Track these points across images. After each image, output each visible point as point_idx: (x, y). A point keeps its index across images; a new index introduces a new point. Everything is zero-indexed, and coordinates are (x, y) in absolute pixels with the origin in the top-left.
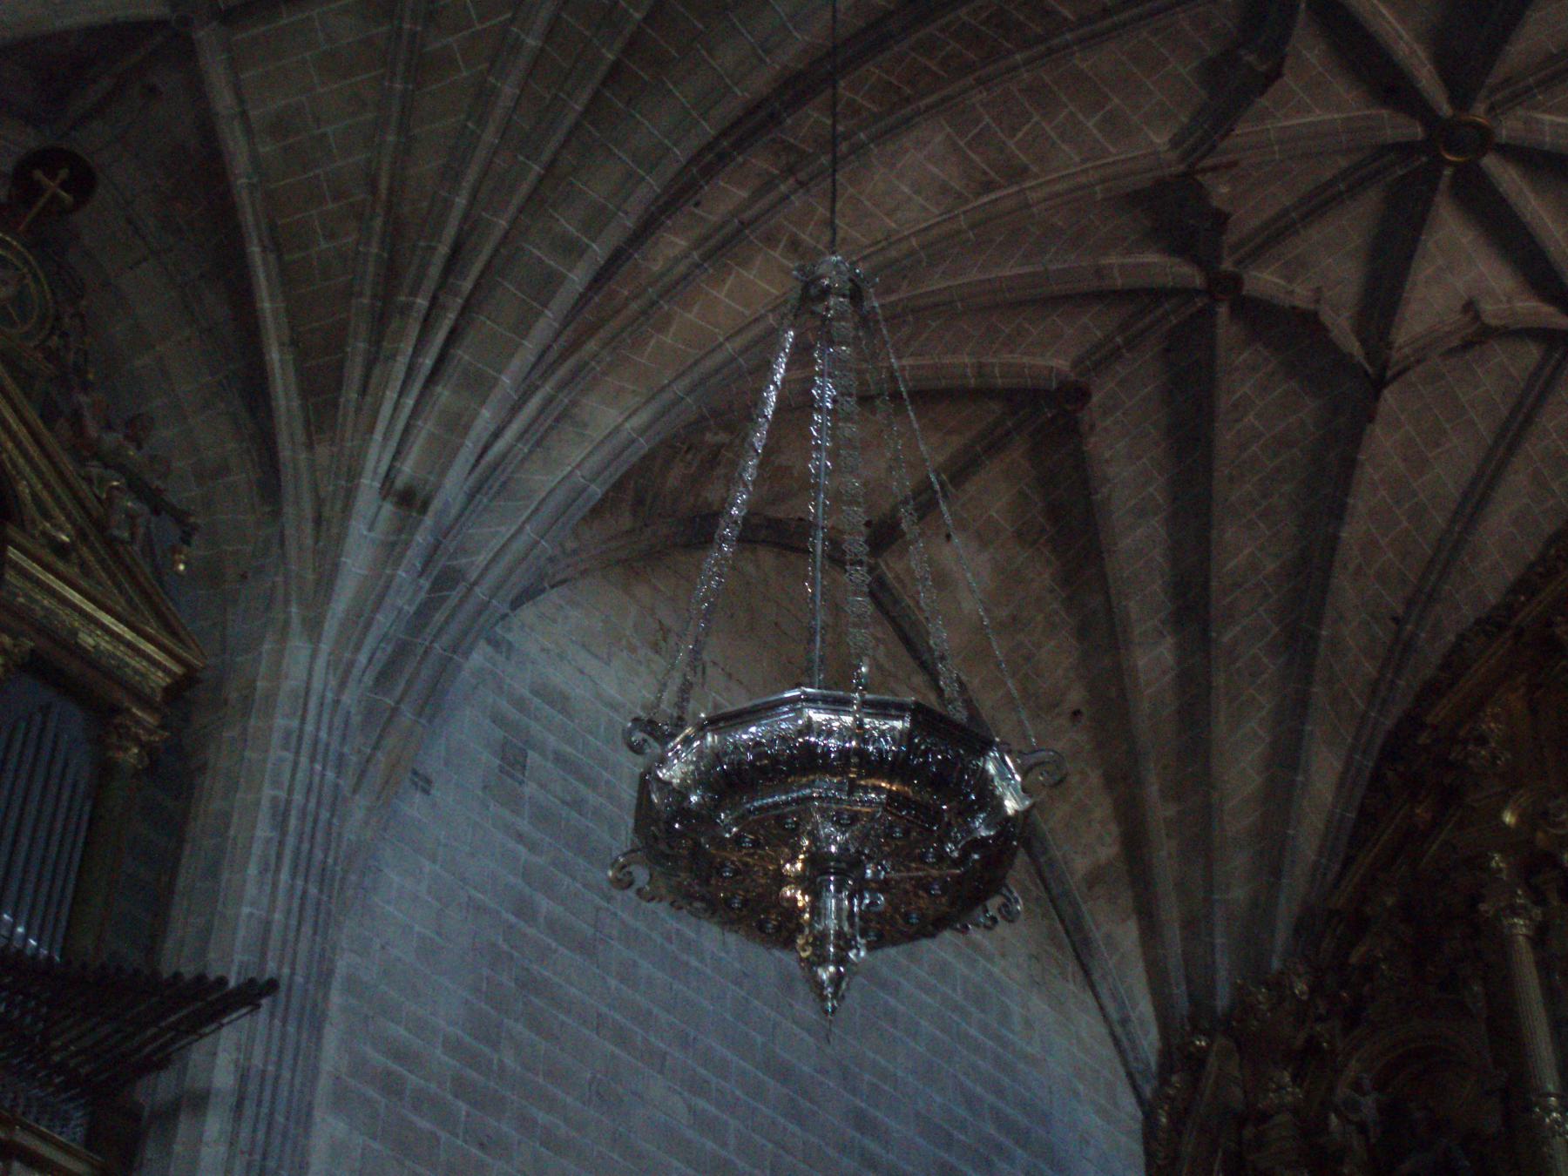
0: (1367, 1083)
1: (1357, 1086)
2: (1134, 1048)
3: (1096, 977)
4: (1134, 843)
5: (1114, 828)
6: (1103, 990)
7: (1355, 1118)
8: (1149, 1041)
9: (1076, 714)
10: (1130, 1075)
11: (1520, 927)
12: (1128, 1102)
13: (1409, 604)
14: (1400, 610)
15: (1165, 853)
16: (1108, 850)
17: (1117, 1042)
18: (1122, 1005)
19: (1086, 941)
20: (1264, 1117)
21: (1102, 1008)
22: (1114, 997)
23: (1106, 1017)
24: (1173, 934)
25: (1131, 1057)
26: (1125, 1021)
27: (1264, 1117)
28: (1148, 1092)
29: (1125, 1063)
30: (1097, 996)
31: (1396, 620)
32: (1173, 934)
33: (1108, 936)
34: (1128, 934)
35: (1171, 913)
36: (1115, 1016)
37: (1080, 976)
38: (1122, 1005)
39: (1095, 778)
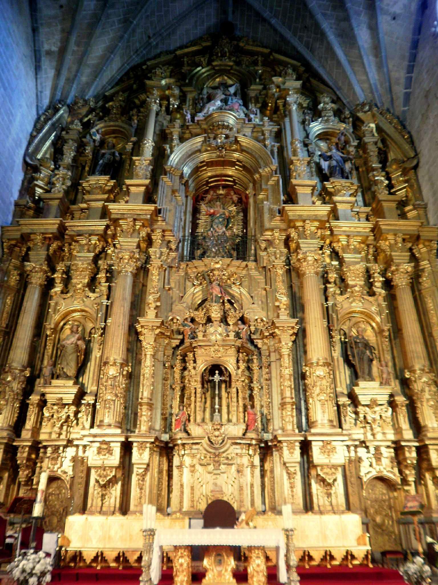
1: (97, 131)
2: (41, 100)
3: (38, 76)
4: (63, 51)
5: (59, 44)
6: (39, 81)
7: (94, 137)
8: (46, 102)
9: (61, 7)
10: (37, 106)
13: (154, 35)
14: (151, 35)
15: (69, 58)
16: (54, 49)
17: (37, 95)
18: (42, 88)
21: (37, 85)
22: (41, 84)
23: (37, 88)
24: (62, 82)
25: (39, 102)
26: (41, 92)
28: (40, 112)
29: (37, 102)
33: (46, 69)
34: (51, 73)
36: (39, 89)
37: (34, 73)
38: (42, 88)
39: (59, 27)
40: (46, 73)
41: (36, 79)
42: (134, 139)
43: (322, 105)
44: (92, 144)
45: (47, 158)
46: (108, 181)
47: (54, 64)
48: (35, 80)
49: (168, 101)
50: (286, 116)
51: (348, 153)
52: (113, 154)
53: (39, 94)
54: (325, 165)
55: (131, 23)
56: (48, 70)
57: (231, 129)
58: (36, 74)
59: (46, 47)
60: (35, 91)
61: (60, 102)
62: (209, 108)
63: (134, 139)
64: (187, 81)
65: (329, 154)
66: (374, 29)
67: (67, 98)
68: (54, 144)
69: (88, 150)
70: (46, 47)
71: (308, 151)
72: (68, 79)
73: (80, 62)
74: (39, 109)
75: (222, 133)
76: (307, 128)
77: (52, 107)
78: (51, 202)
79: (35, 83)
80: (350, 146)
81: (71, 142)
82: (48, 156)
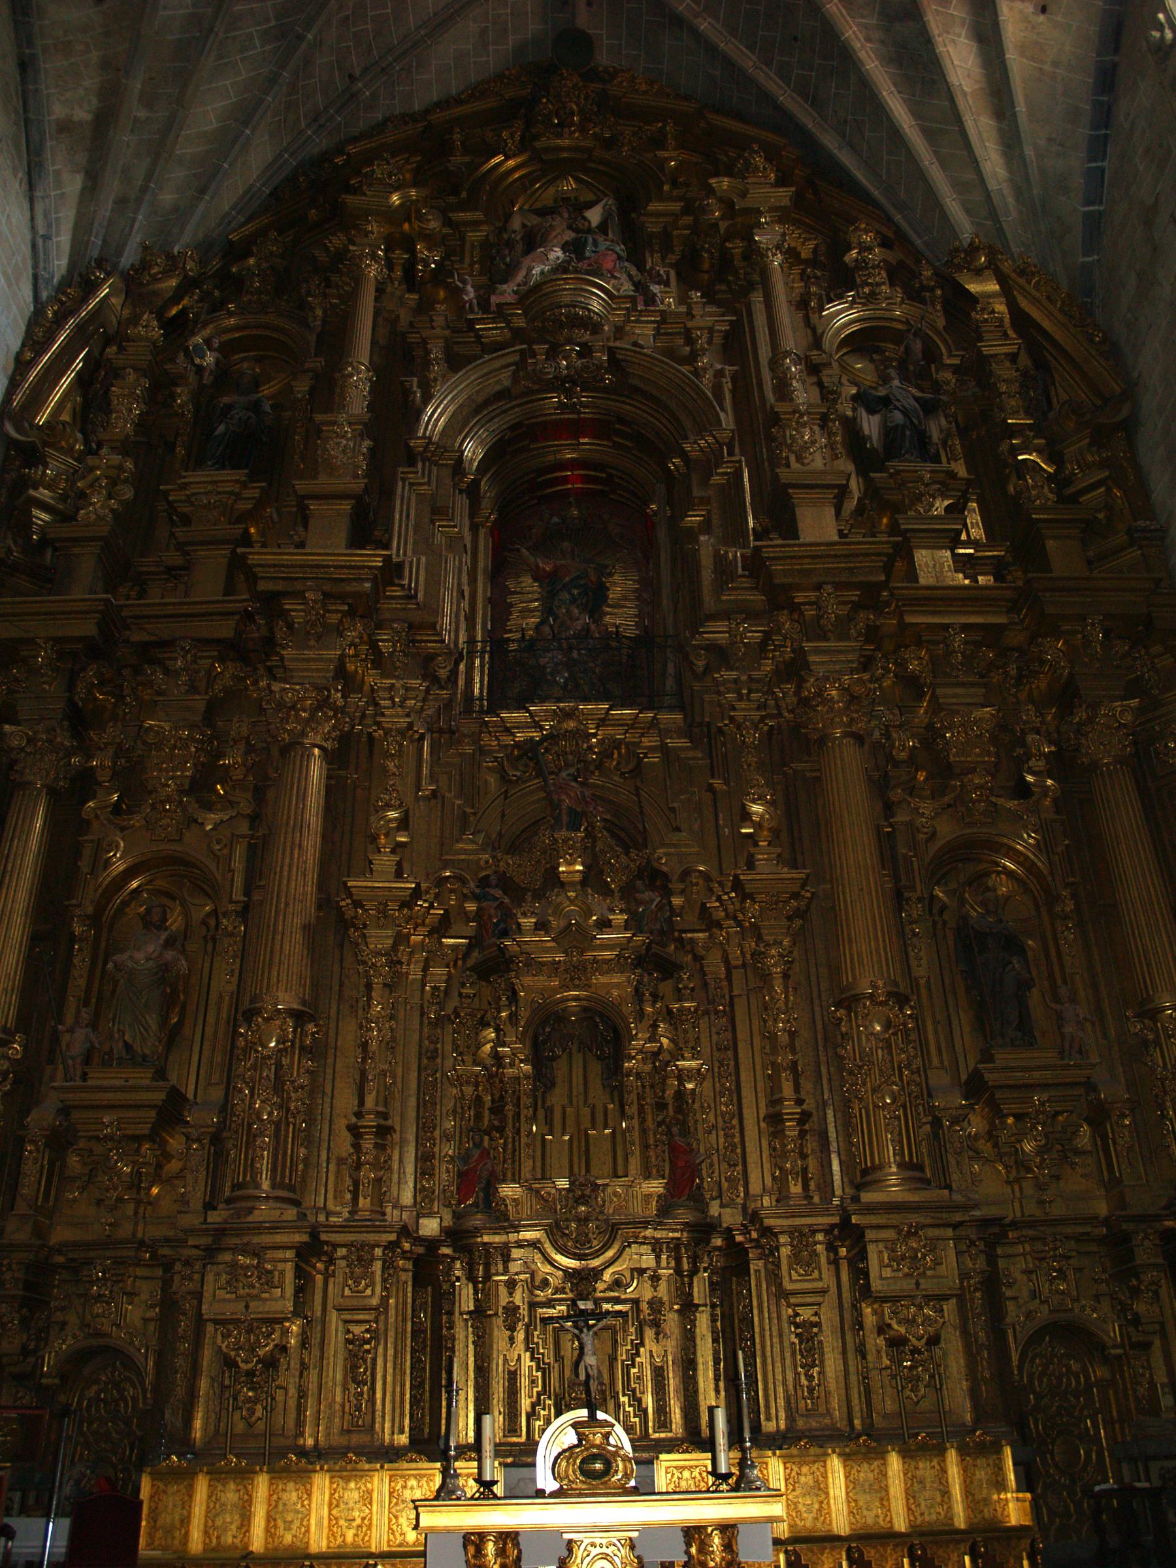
1: (208, 342)
2: (46, 261)
3: (38, 194)
7: (197, 361)
8: (60, 265)
10: (35, 277)
12: (27, 292)
13: (366, 70)
14: (357, 73)
16: (82, 115)
17: (34, 246)
18: (49, 226)
19: (40, 165)
21: (32, 219)
22: (46, 214)
23: (33, 228)
24: (105, 209)
26: (47, 238)
28: (44, 295)
29: (35, 266)
30: (32, 209)
31: (351, 76)
33: (58, 173)
34: (74, 184)
36: (41, 231)
37: (25, 186)
38: (49, 226)
39: (95, 55)
40: (59, 184)
41: (32, 201)
42: (319, 363)
44: (192, 378)
45: (64, 423)
46: (244, 485)
47: (82, 158)
48: (26, 206)
49: (412, 251)
50: (751, 286)
51: (937, 387)
52: (256, 407)
53: (40, 241)
54: (870, 425)
55: (300, 38)
56: (66, 176)
57: (596, 328)
58: (31, 187)
59: (58, 111)
60: (29, 237)
61: (100, 263)
62: (530, 269)
63: (319, 363)
64: (464, 195)
65: (882, 392)
67: (119, 253)
68: (81, 380)
69: (182, 396)
70: (58, 111)
71: (820, 384)
72: (122, 202)
75: (570, 341)
76: (814, 318)
77: (76, 278)
79: (28, 214)
81: (132, 377)
82: (65, 417)
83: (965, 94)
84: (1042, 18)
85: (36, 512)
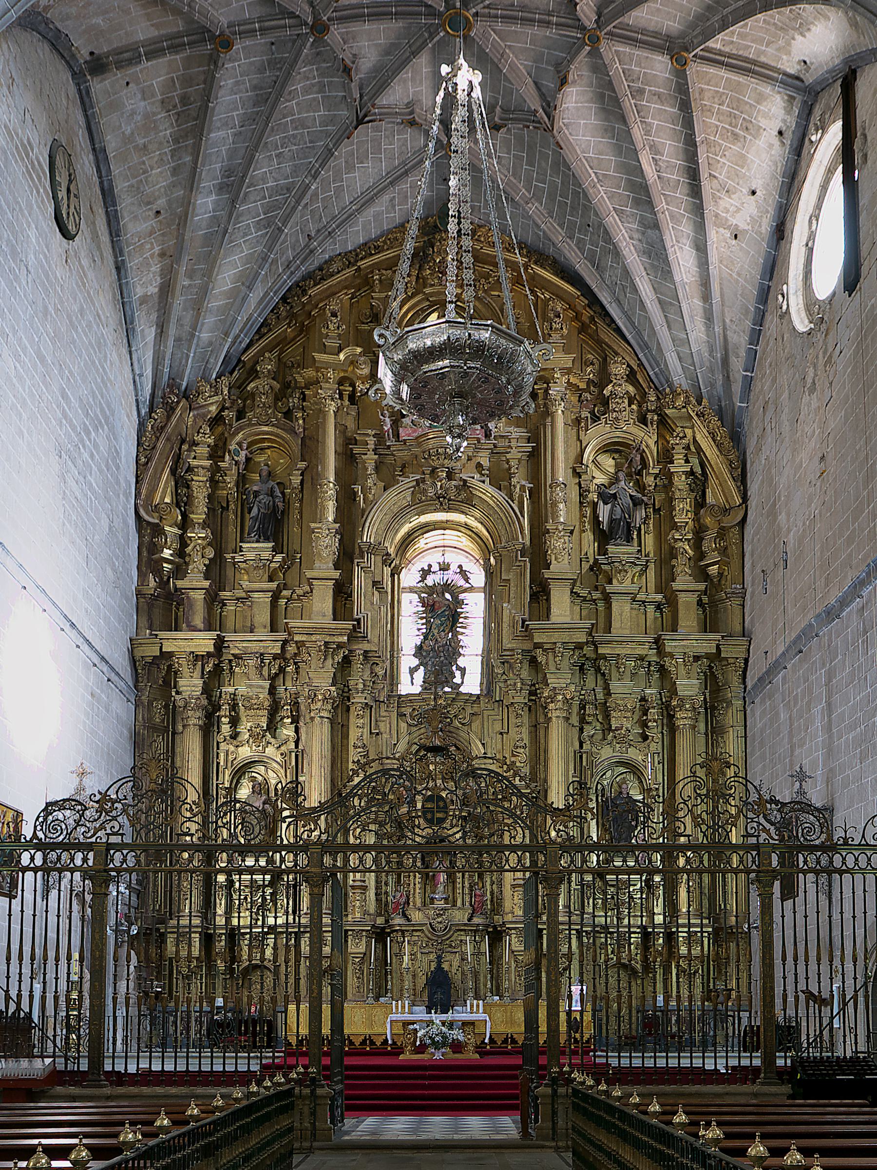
0: (245, 446)
6: (134, 357)
10: (137, 400)
11: (332, 407)
17: (134, 382)
20: (195, 444)
26: (141, 375)
27: (195, 444)
29: (136, 396)
30: (131, 359)
32: (171, 342)
34: (151, 334)
35: (172, 331)
40: (143, 338)
42: (302, 465)
43: (610, 387)
48: (124, 351)
49: (353, 385)
52: (271, 493)
56: (147, 331)
59: (139, 291)
60: (131, 377)
63: (302, 465)
66: (701, 248)
70: (139, 291)
71: (580, 484)
72: (178, 340)
73: (198, 306)
74: (141, 406)
78: (192, 593)
80: (648, 474)
81: (201, 471)
83: (684, 285)
84: (734, 242)
85: (165, 565)
